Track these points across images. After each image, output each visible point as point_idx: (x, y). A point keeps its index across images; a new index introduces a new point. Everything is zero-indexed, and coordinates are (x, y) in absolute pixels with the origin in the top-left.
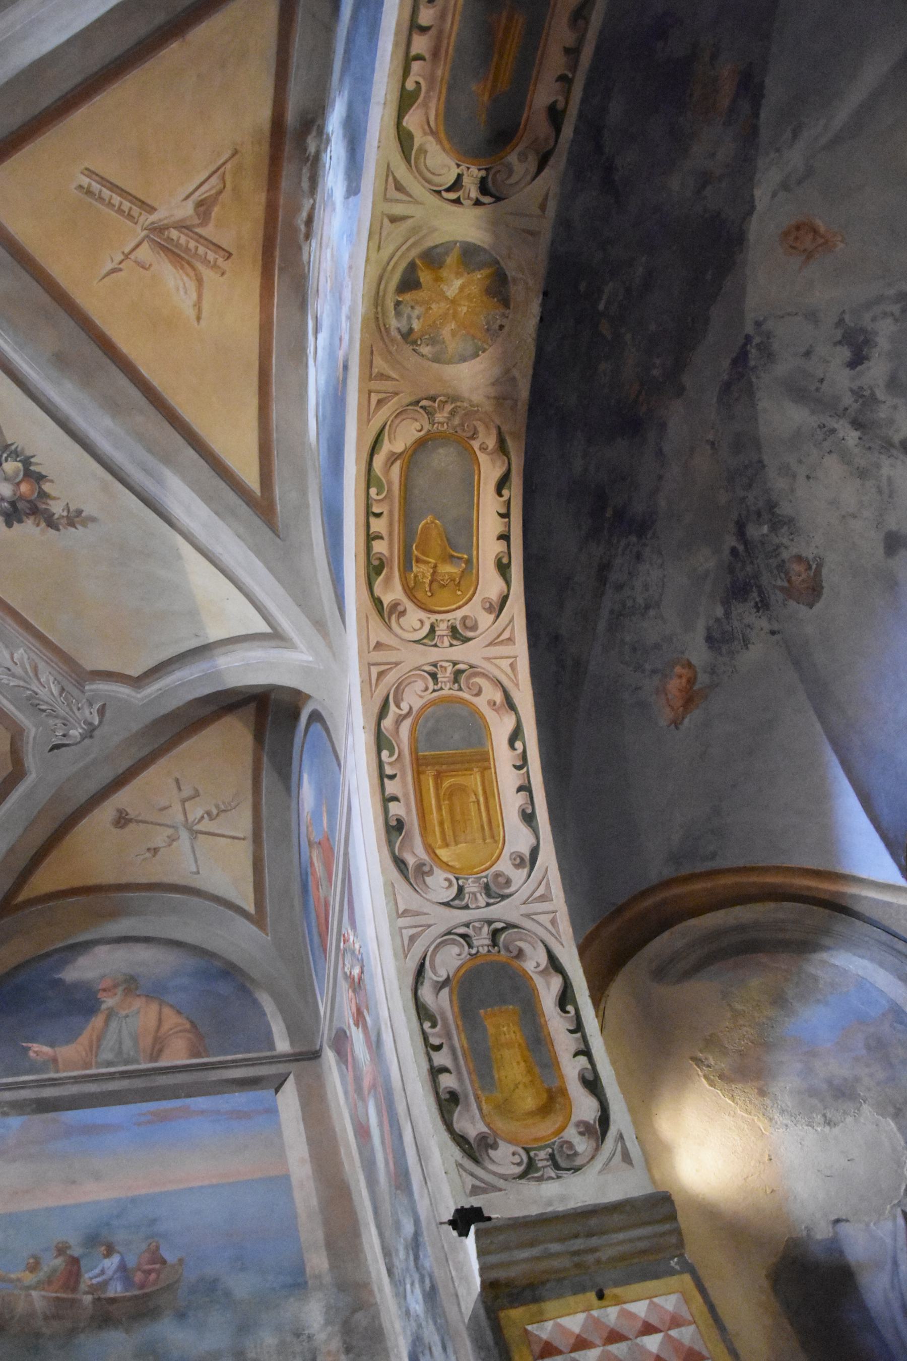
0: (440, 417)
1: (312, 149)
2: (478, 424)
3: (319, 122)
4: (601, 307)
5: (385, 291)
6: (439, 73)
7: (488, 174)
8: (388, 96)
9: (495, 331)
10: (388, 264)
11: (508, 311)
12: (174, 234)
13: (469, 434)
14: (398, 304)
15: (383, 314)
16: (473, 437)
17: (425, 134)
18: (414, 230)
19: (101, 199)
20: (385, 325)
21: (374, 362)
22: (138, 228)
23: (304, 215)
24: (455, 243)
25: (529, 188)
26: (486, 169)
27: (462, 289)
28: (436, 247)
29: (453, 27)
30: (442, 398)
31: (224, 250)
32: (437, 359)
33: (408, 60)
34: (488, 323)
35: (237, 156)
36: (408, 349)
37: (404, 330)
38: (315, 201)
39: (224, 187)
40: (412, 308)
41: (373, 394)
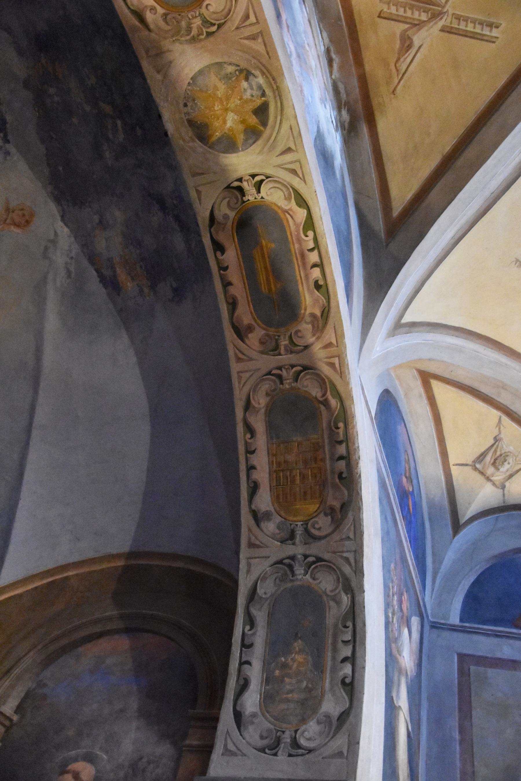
0: (197, 22)
1: (344, 113)
2: (168, 28)
3: (345, 132)
4: (119, 123)
5: (276, 102)
6: (297, 246)
7: (242, 199)
8: (321, 223)
9: (188, 100)
10: (281, 120)
11: (187, 118)
12: (424, 17)
13: (169, 17)
14: (263, 94)
15: (271, 84)
16: (165, 15)
17: (291, 209)
18: (273, 147)
19: (481, 23)
20: (266, 76)
21: (263, 47)
22: (451, 12)
23: (335, 66)
24: (243, 150)
25: (212, 202)
26: (244, 202)
27: (225, 122)
28: (254, 142)
29: (299, 273)
30: (202, 37)
31: (385, 18)
32: (220, 65)
33: (317, 246)
34: (196, 104)
35: (391, 91)
36: (243, 65)
37: (251, 78)
38: (331, 78)
39: (395, 66)
40: (252, 96)
41: (255, 21)
